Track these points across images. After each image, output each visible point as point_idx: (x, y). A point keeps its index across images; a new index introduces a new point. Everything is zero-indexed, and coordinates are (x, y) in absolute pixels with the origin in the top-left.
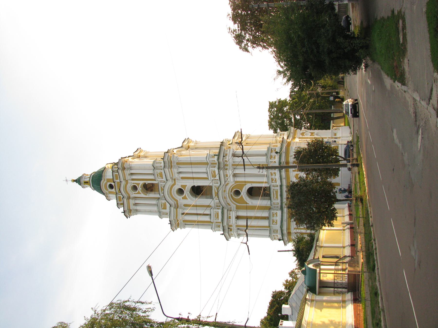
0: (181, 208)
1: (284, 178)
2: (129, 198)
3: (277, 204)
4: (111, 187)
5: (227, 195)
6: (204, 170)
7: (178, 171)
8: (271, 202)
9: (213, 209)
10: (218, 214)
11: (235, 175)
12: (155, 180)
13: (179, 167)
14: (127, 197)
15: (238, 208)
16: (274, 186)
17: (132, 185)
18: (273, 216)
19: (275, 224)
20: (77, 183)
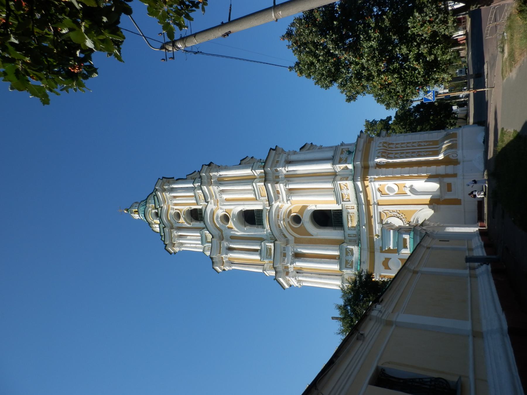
0: (227, 240)
1: (361, 192)
2: (172, 228)
3: (353, 237)
8: (345, 233)
10: (270, 249)
12: (197, 204)
13: (220, 184)
14: (169, 226)
15: (298, 242)
17: (175, 211)
18: (347, 255)
19: (350, 267)
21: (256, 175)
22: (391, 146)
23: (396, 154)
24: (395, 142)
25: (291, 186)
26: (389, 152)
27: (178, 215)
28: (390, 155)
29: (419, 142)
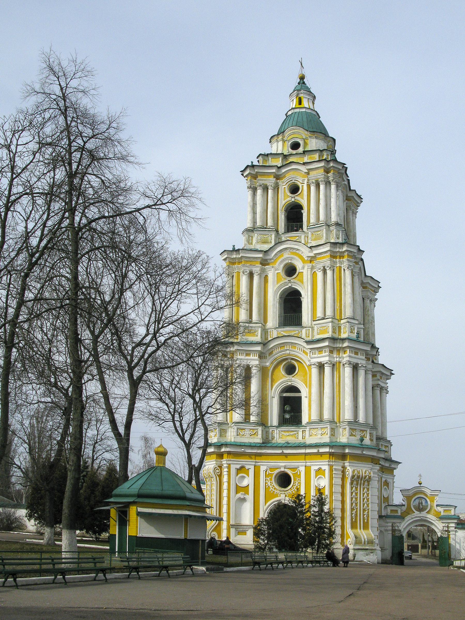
0: (263, 271)
4: (295, 146)
5: (288, 352)
6: (329, 312)
7: (328, 269)
9: (261, 327)
11: (321, 367)
15: (263, 371)
16: (304, 433)
20: (299, 83)
21: (342, 321)
22: (366, 483)
23: (356, 488)
24: (370, 487)
25: (327, 370)
26: (359, 482)
27: (295, 189)
28: (355, 482)
29: (368, 509)
